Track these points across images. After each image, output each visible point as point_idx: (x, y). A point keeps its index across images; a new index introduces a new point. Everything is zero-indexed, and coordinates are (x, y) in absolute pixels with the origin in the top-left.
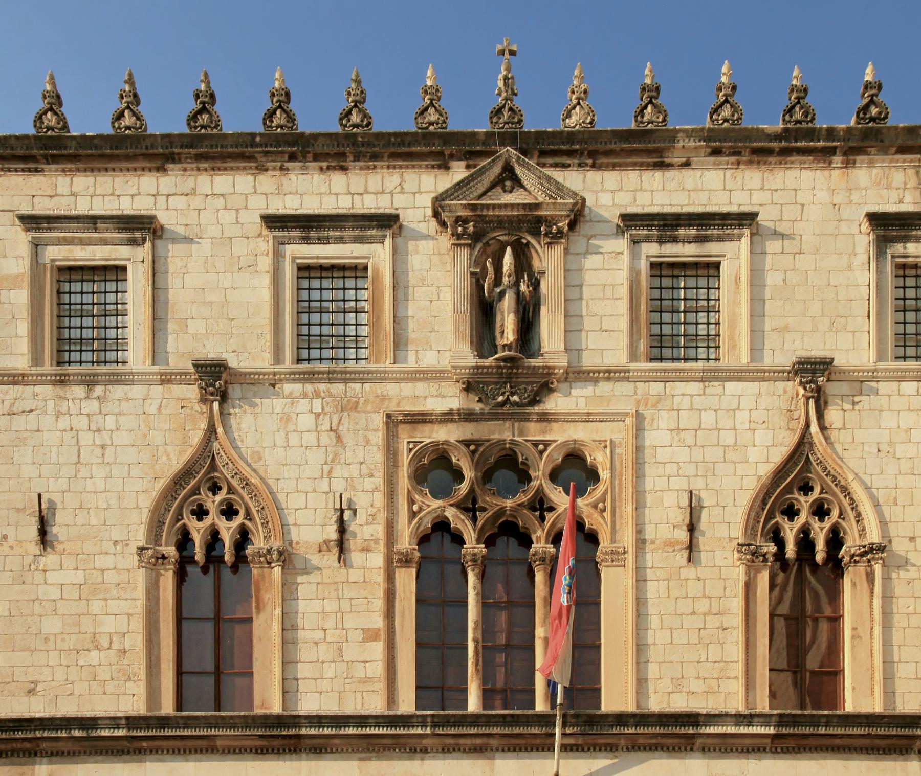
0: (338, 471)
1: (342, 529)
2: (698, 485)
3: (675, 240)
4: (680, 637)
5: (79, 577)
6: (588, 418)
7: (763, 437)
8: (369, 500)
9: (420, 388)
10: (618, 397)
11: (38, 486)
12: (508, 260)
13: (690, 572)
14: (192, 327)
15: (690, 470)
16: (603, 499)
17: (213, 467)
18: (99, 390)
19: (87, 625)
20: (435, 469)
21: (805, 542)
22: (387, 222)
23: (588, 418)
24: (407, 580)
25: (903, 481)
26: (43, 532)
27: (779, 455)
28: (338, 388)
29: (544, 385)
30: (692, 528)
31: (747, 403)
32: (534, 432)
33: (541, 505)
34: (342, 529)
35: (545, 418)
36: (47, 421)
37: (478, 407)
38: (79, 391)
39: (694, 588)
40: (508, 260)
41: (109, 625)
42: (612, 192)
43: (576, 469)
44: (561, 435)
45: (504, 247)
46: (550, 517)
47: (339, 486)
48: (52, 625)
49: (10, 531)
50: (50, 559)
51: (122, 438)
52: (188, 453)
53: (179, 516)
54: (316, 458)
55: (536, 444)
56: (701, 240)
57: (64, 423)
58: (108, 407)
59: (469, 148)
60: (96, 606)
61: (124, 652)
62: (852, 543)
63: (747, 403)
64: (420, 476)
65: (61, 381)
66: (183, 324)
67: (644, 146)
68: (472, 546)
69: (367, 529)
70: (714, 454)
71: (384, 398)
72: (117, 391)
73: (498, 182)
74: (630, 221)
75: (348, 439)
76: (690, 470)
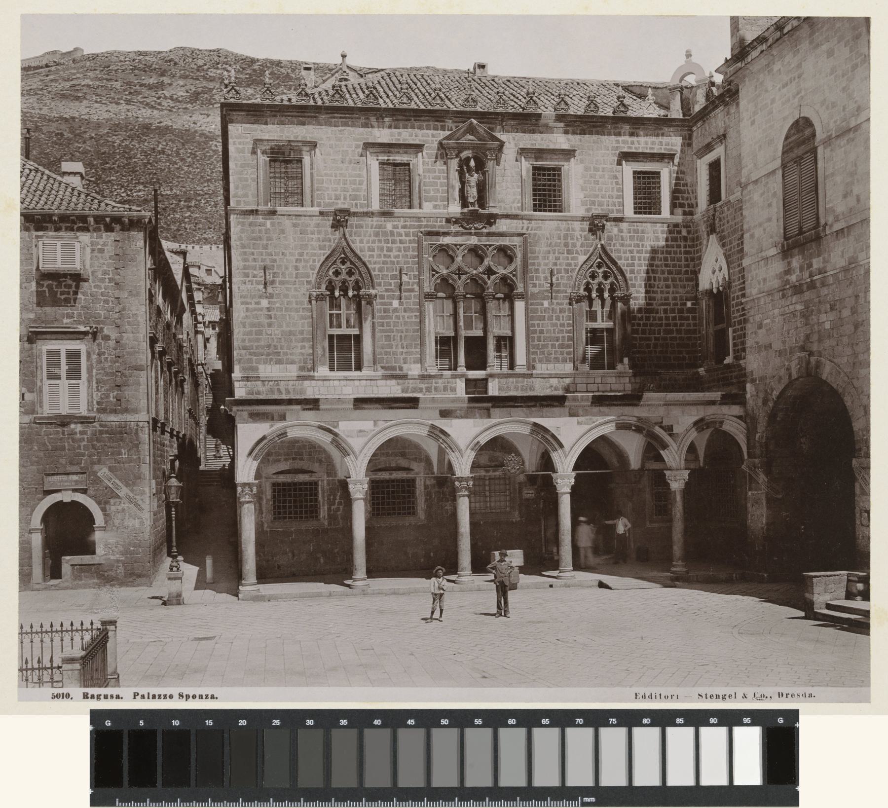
16: (515, 270)
29: (491, 219)
33: (490, 272)
46: (493, 277)
55: (485, 246)
67: (527, 121)
74: (523, 152)
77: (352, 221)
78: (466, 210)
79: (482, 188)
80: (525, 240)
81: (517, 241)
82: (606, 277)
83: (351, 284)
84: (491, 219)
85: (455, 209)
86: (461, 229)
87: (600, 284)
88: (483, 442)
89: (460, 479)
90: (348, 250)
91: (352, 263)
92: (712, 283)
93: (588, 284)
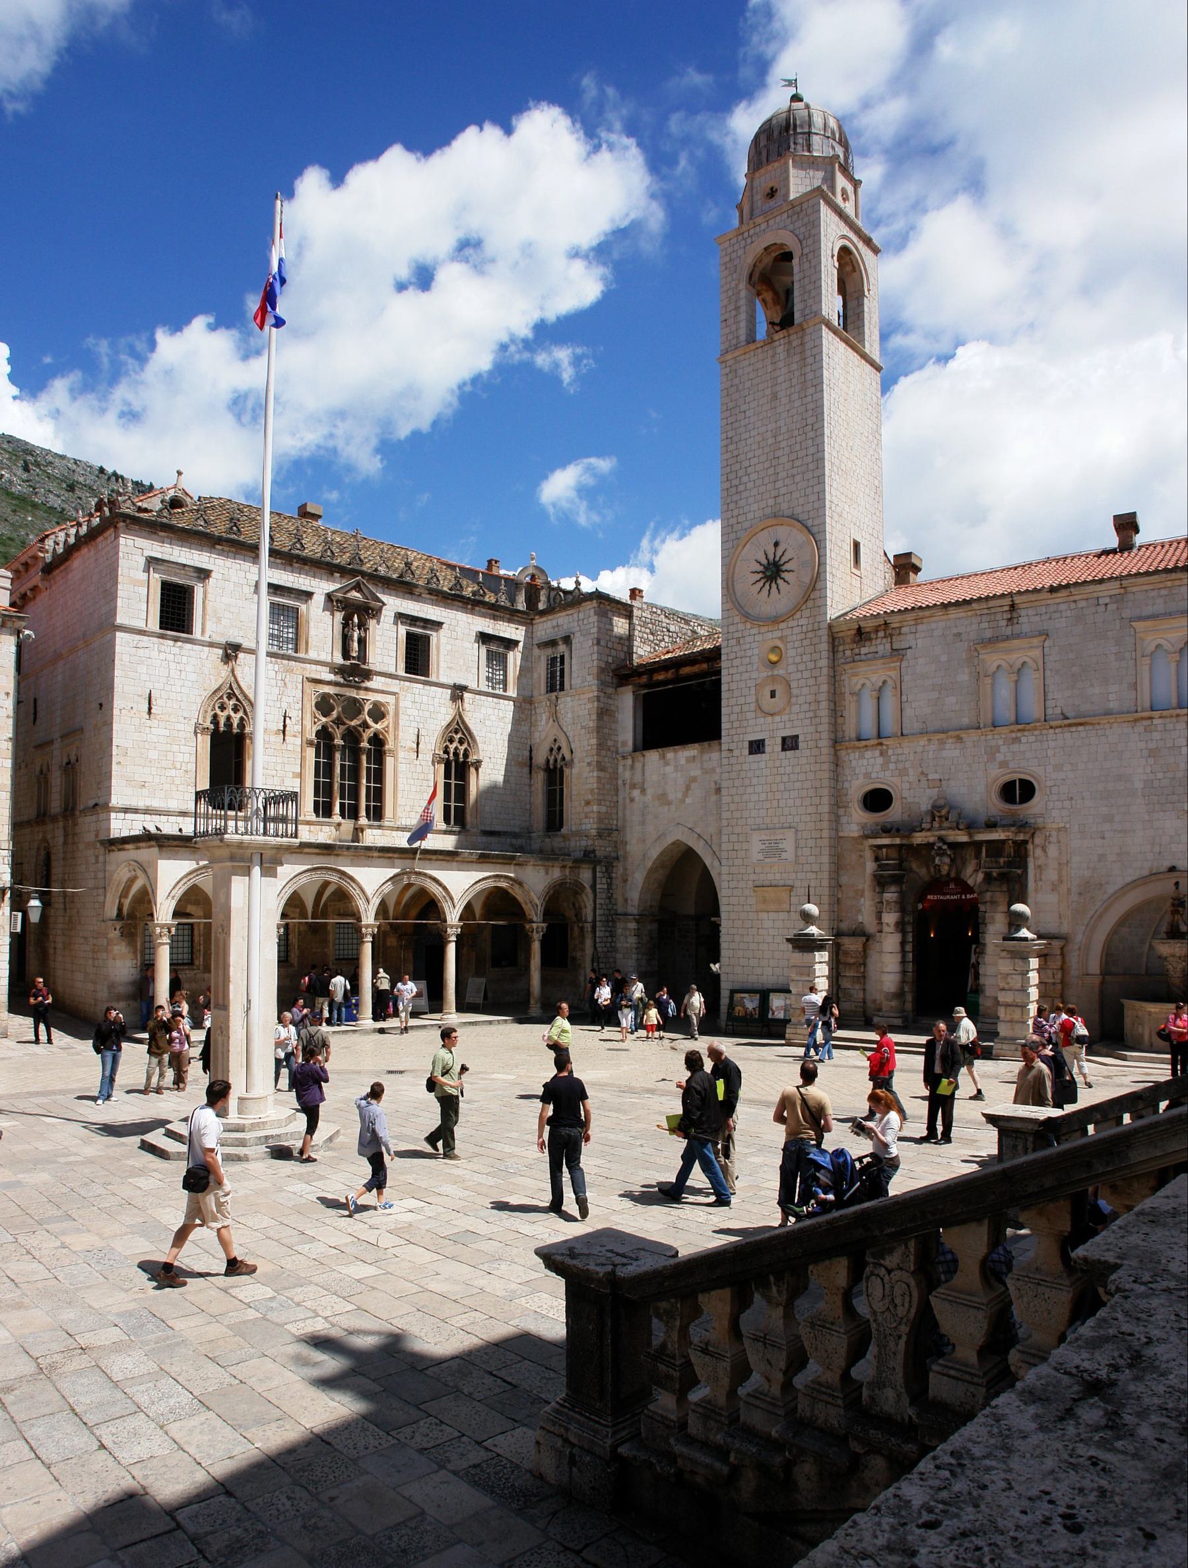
0: (284, 699)
1: (285, 726)
2: (421, 726)
3: (415, 626)
4: (414, 789)
5: (167, 733)
6: (383, 692)
7: (443, 710)
8: (295, 714)
9: (319, 668)
10: (394, 685)
11: (150, 686)
12: (356, 620)
13: (417, 762)
14: (224, 621)
15: (418, 719)
17: (231, 688)
18: (179, 644)
19: (170, 756)
20: (324, 705)
21: (456, 754)
22: (309, 595)
23: (383, 692)
24: (311, 752)
25: (489, 735)
26: (150, 709)
27: (449, 718)
28: (286, 662)
29: (367, 675)
30: (418, 744)
31: (439, 695)
32: (362, 695)
33: (365, 725)
34: (285, 726)
35: (367, 689)
36: (155, 654)
37: (342, 680)
38: (171, 643)
39: (419, 769)
40: (356, 620)
41: (180, 758)
42: (393, 604)
43: (378, 713)
44: (373, 697)
45: (355, 614)
47: (284, 706)
48: (153, 755)
49: (134, 706)
50: (154, 723)
51: (189, 668)
52: (221, 681)
53: (214, 709)
54: (277, 691)
56: (424, 628)
57: (162, 656)
58: (184, 652)
59: (343, 571)
60: (175, 748)
61: (186, 771)
62: (472, 758)
63: (439, 695)
64: (318, 706)
65: (162, 637)
66: (219, 620)
67: (404, 586)
68: (338, 741)
69: (293, 727)
70: (427, 714)
71: (304, 669)
72: (189, 646)
73: (354, 588)
74: (401, 617)
75: (289, 685)
76: (418, 719)
77: (241, 655)
78: (348, 663)
79: (362, 642)
80: (397, 700)
81: (389, 699)
82: (461, 742)
83: (235, 722)
84: (367, 675)
85: (339, 659)
86: (342, 680)
87: (456, 748)
88: (386, 891)
89: (367, 926)
90: (235, 686)
91: (238, 700)
92: (548, 761)
93: (447, 747)
